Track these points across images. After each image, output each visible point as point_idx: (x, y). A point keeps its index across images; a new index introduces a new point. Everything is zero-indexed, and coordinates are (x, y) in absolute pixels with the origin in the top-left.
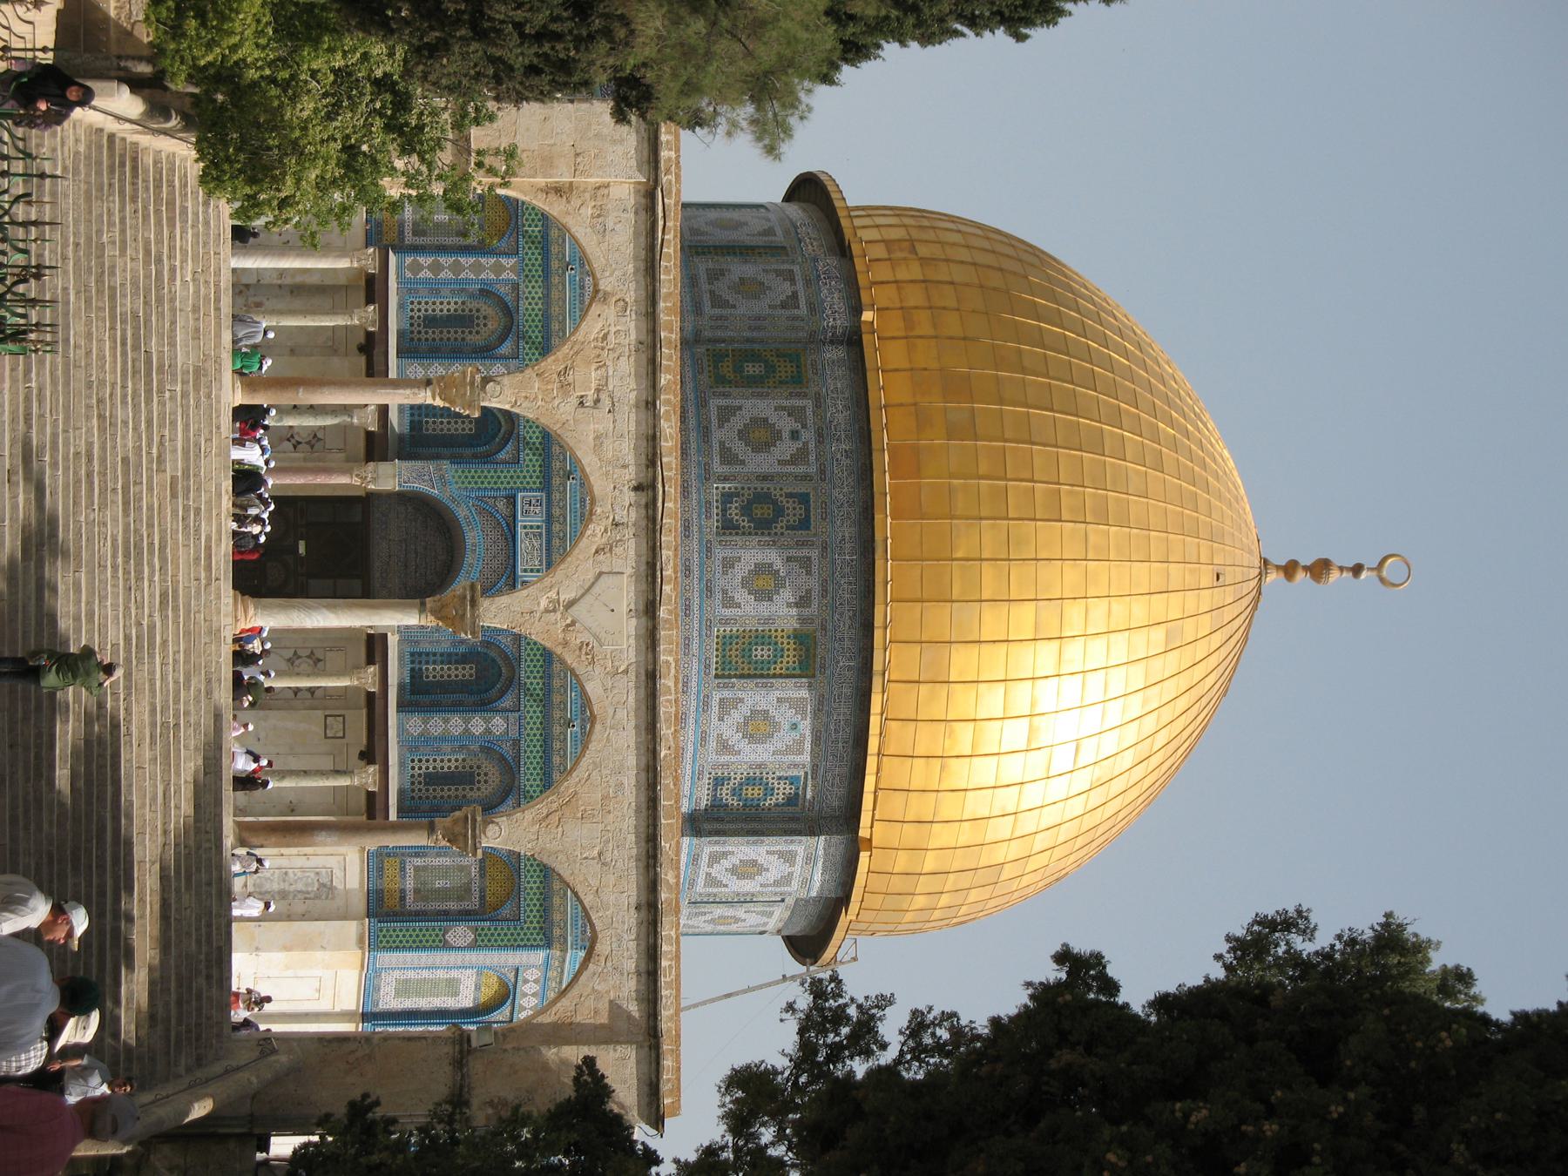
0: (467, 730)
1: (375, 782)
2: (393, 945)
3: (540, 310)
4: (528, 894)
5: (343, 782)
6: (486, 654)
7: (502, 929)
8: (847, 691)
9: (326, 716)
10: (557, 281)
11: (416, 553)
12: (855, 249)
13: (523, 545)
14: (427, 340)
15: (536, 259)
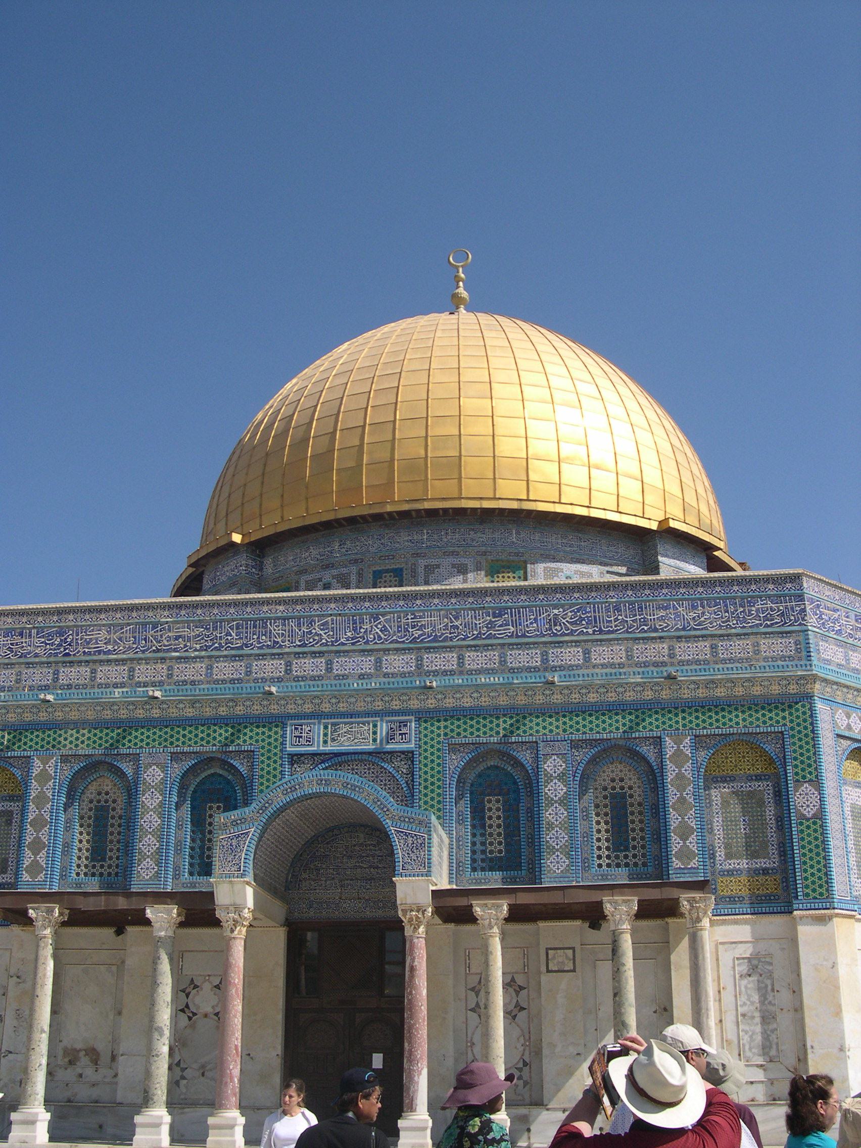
0: (561, 802)
1: (625, 901)
2: (824, 879)
3: (89, 732)
4: (751, 723)
5: (627, 944)
6: (472, 785)
7: (795, 751)
8: (537, 536)
9: (548, 971)
10: (60, 714)
11: (356, 867)
12: (193, 560)
13: (345, 744)
14: (118, 858)
15: (37, 736)
